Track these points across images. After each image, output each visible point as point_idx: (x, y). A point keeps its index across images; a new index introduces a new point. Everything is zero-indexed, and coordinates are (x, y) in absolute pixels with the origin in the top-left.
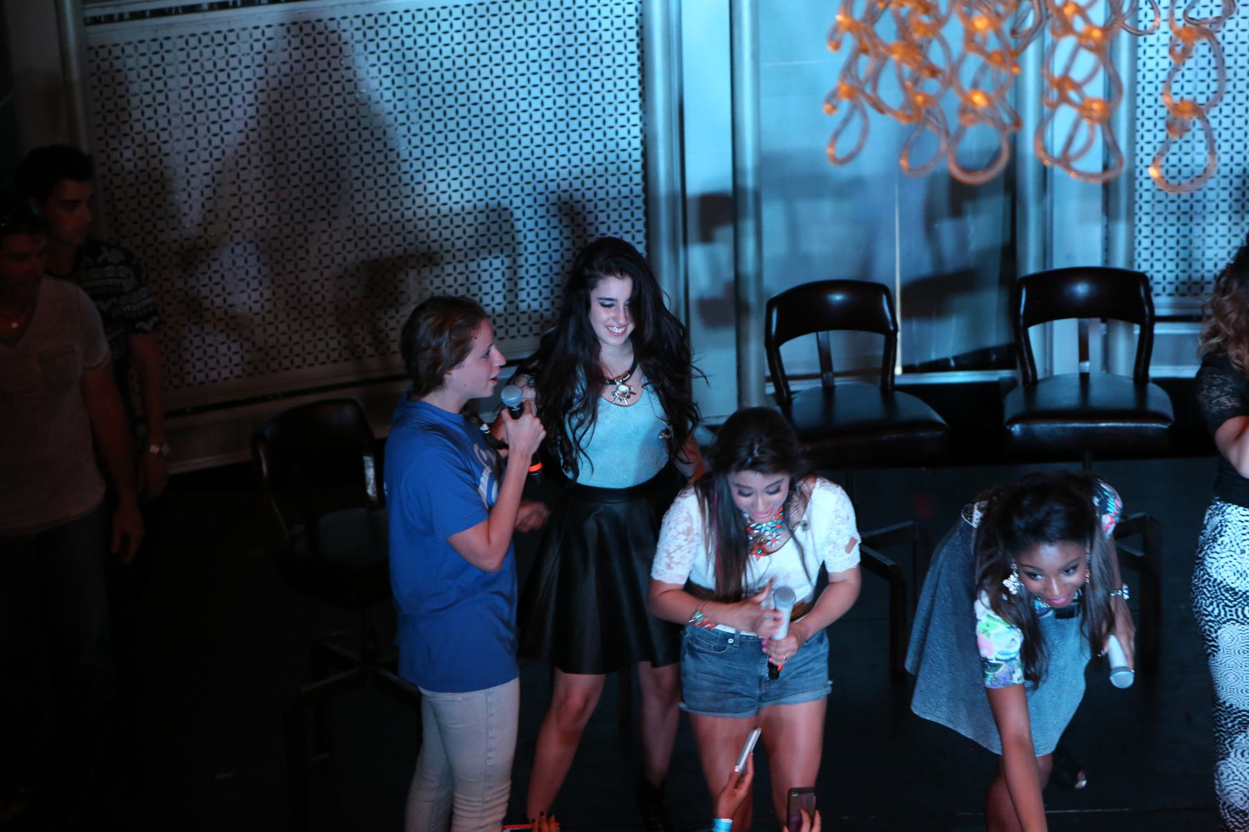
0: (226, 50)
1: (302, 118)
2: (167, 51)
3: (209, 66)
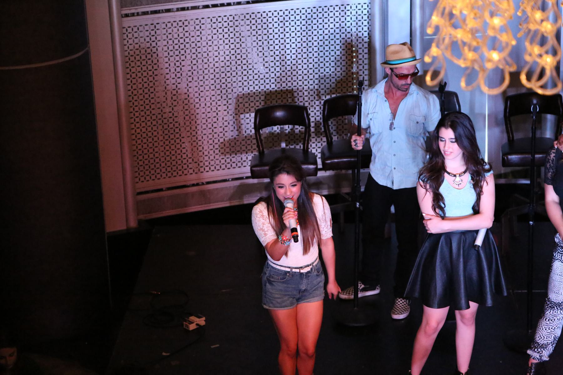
0: (184, 29)
1: (216, 59)
2: (158, 29)
3: (176, 36)
